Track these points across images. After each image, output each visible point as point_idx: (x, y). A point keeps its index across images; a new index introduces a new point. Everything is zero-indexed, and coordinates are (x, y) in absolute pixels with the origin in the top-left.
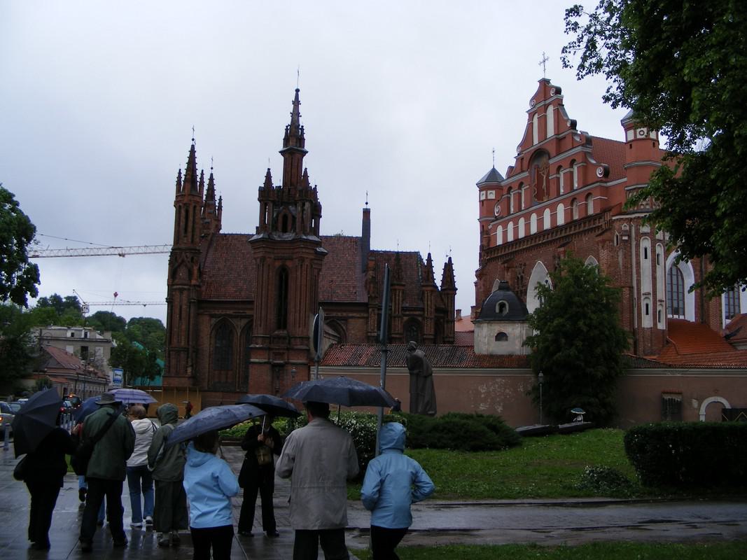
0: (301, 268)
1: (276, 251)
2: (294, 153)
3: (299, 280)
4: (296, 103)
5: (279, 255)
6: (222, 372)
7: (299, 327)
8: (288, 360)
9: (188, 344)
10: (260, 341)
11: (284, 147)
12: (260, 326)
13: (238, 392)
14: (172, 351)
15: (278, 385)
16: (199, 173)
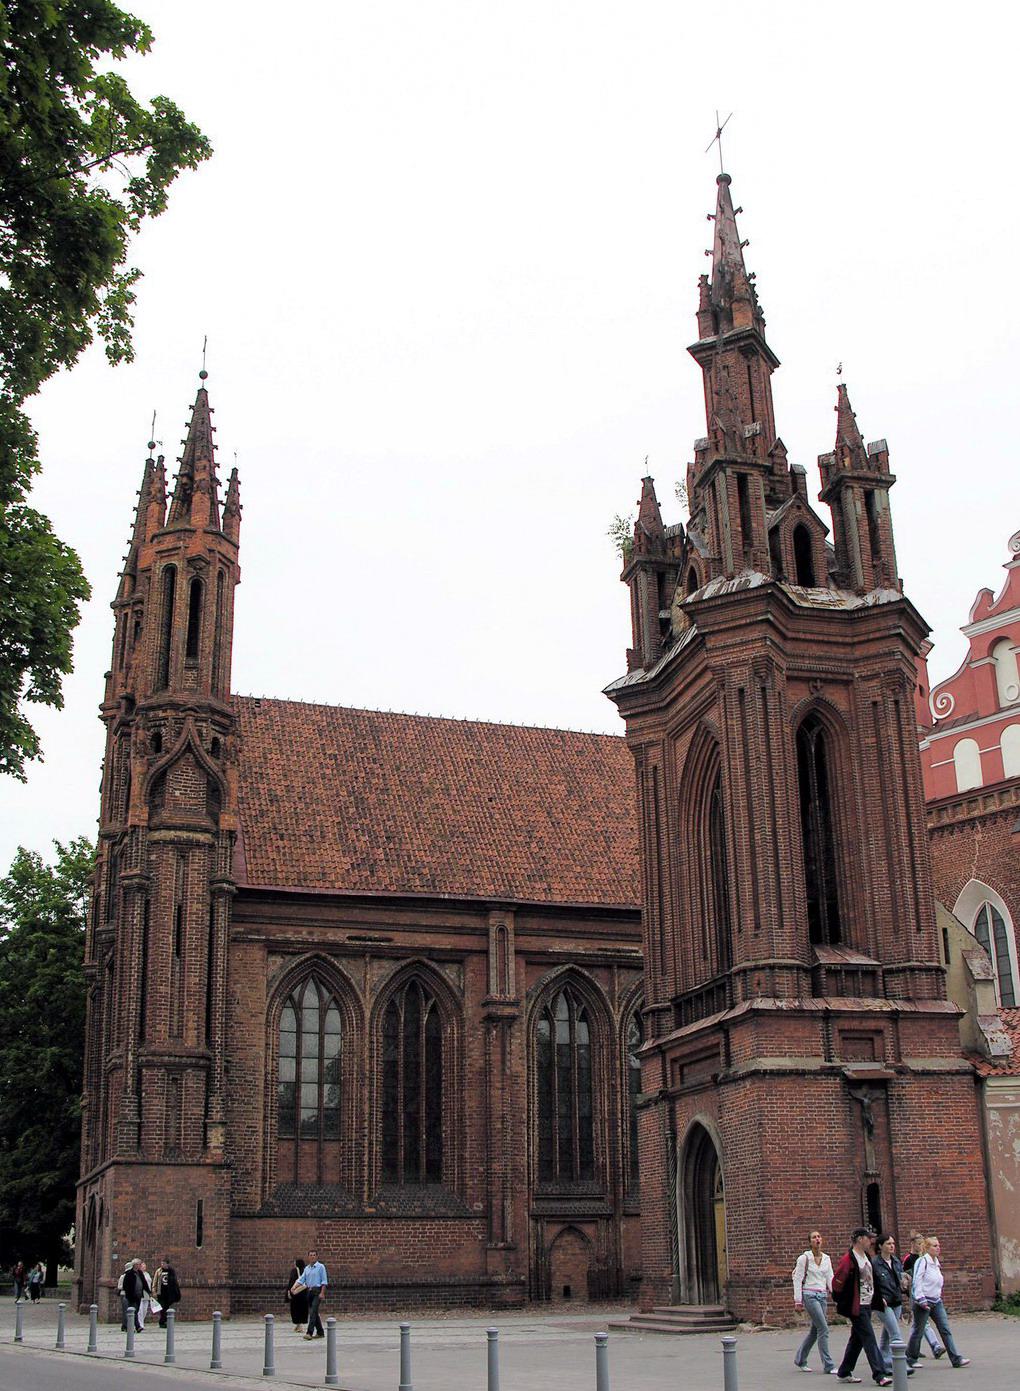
0: (898, 711)
1: (789, 647)
2: (755, 353)
3: (896, 757)
4: (726, 211)
5: (807, 664)
6: (306, 1147)
7: (919, 930)
8: (898, 1056)
9: (209, 1043)
10: (785, 981)
11: (702, 334)
12: (781, 926)
13: (371, 1217)
14: (150, 1065)
15: (872, 1161)
16: (223, 474)
